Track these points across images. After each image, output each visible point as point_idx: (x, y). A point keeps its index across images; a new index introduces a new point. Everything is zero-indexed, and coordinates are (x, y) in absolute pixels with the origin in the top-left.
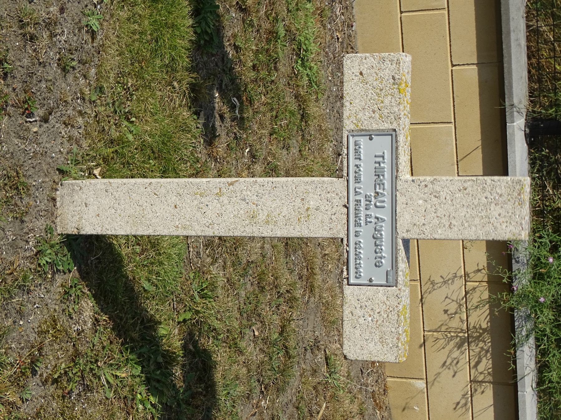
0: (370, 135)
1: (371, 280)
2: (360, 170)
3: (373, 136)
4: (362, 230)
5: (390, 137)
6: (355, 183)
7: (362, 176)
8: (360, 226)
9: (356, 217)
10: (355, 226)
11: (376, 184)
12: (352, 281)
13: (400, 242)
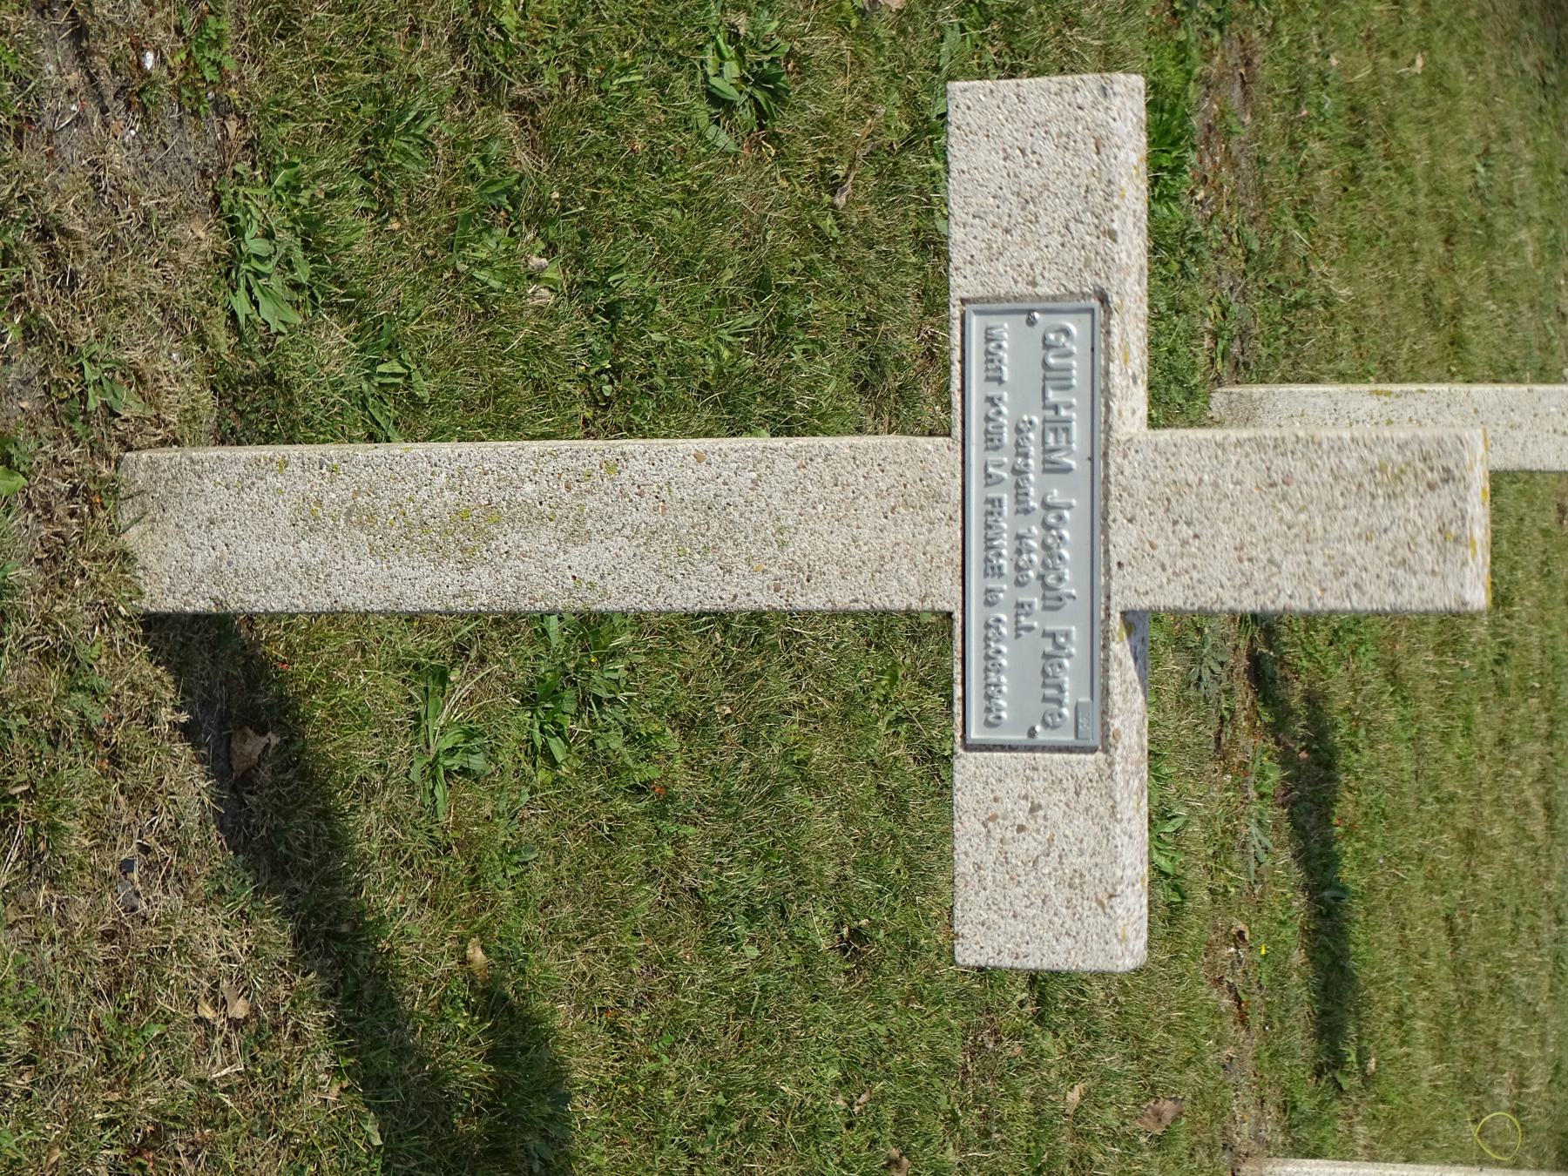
0: (1030, 312)
1: (1032, 733)
2: (999, 413)
3: (1036, 315)
4: (1005, 587)
5: (1088, 317)
6: (987, 449)
7: (1005, 429)
8: (1001, 575)
9: (988, 548)
10: (986, 575)
11: (1047, 430)
12: (975, 735)
13: (1116, 622)
